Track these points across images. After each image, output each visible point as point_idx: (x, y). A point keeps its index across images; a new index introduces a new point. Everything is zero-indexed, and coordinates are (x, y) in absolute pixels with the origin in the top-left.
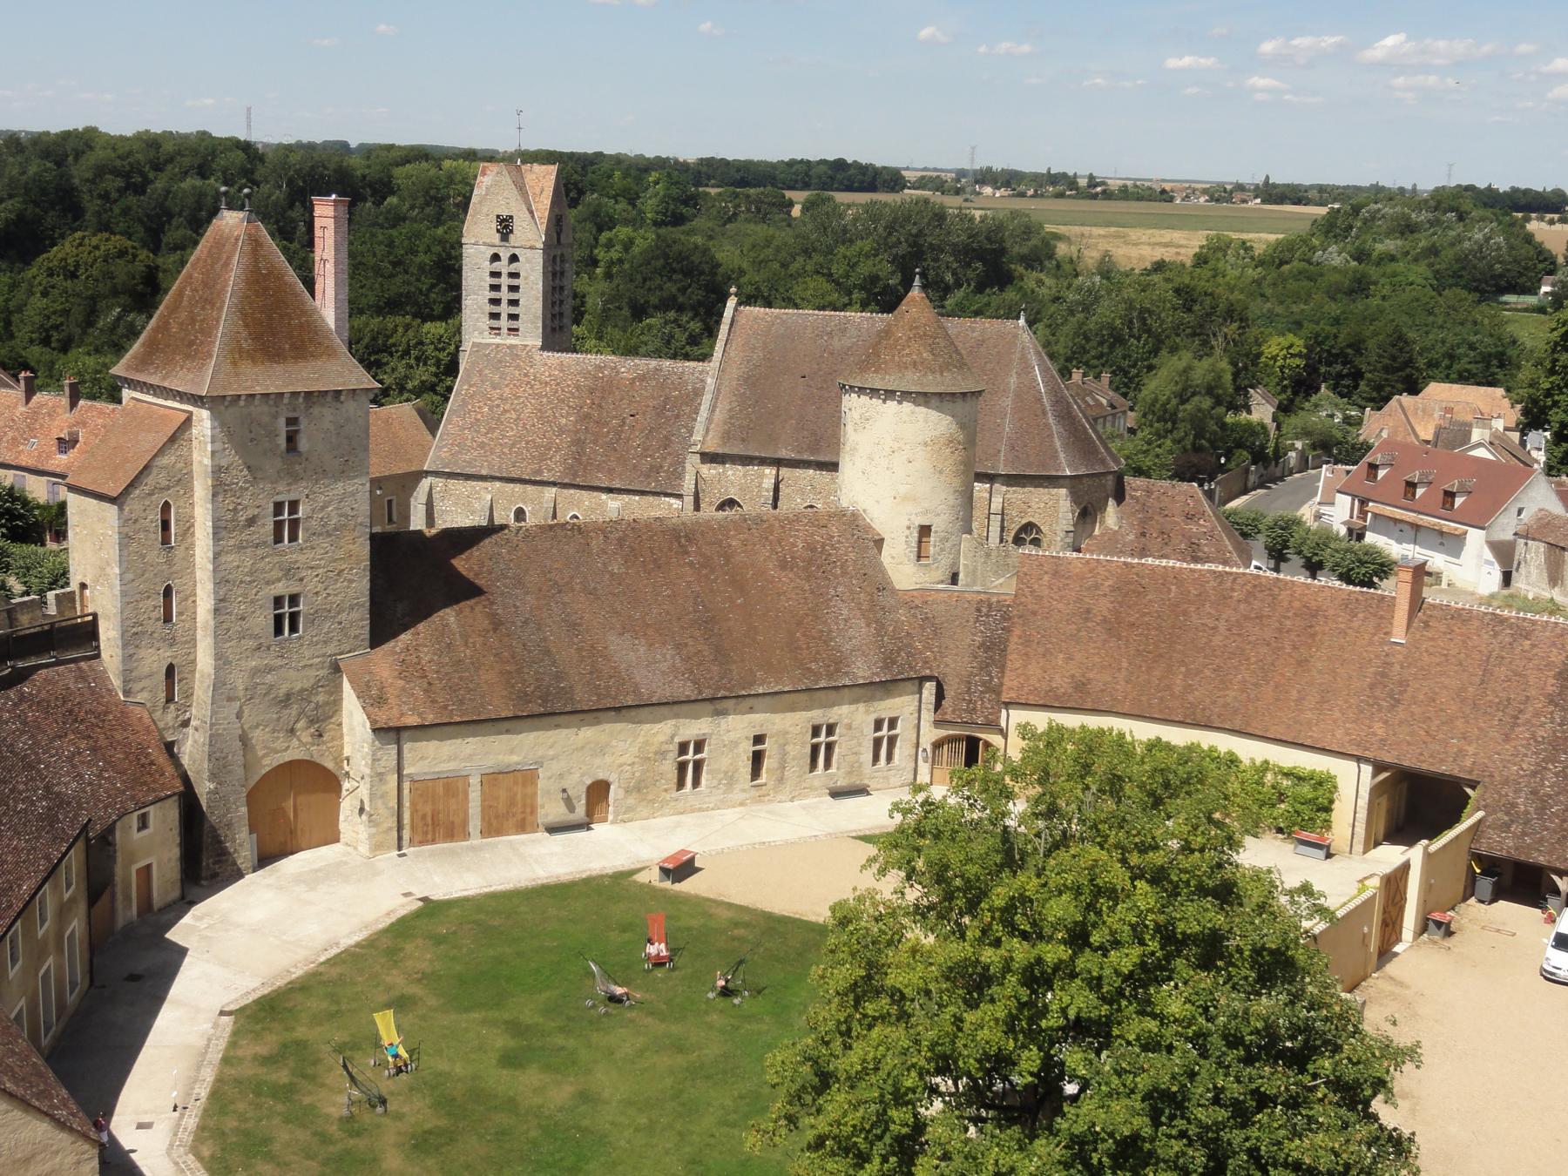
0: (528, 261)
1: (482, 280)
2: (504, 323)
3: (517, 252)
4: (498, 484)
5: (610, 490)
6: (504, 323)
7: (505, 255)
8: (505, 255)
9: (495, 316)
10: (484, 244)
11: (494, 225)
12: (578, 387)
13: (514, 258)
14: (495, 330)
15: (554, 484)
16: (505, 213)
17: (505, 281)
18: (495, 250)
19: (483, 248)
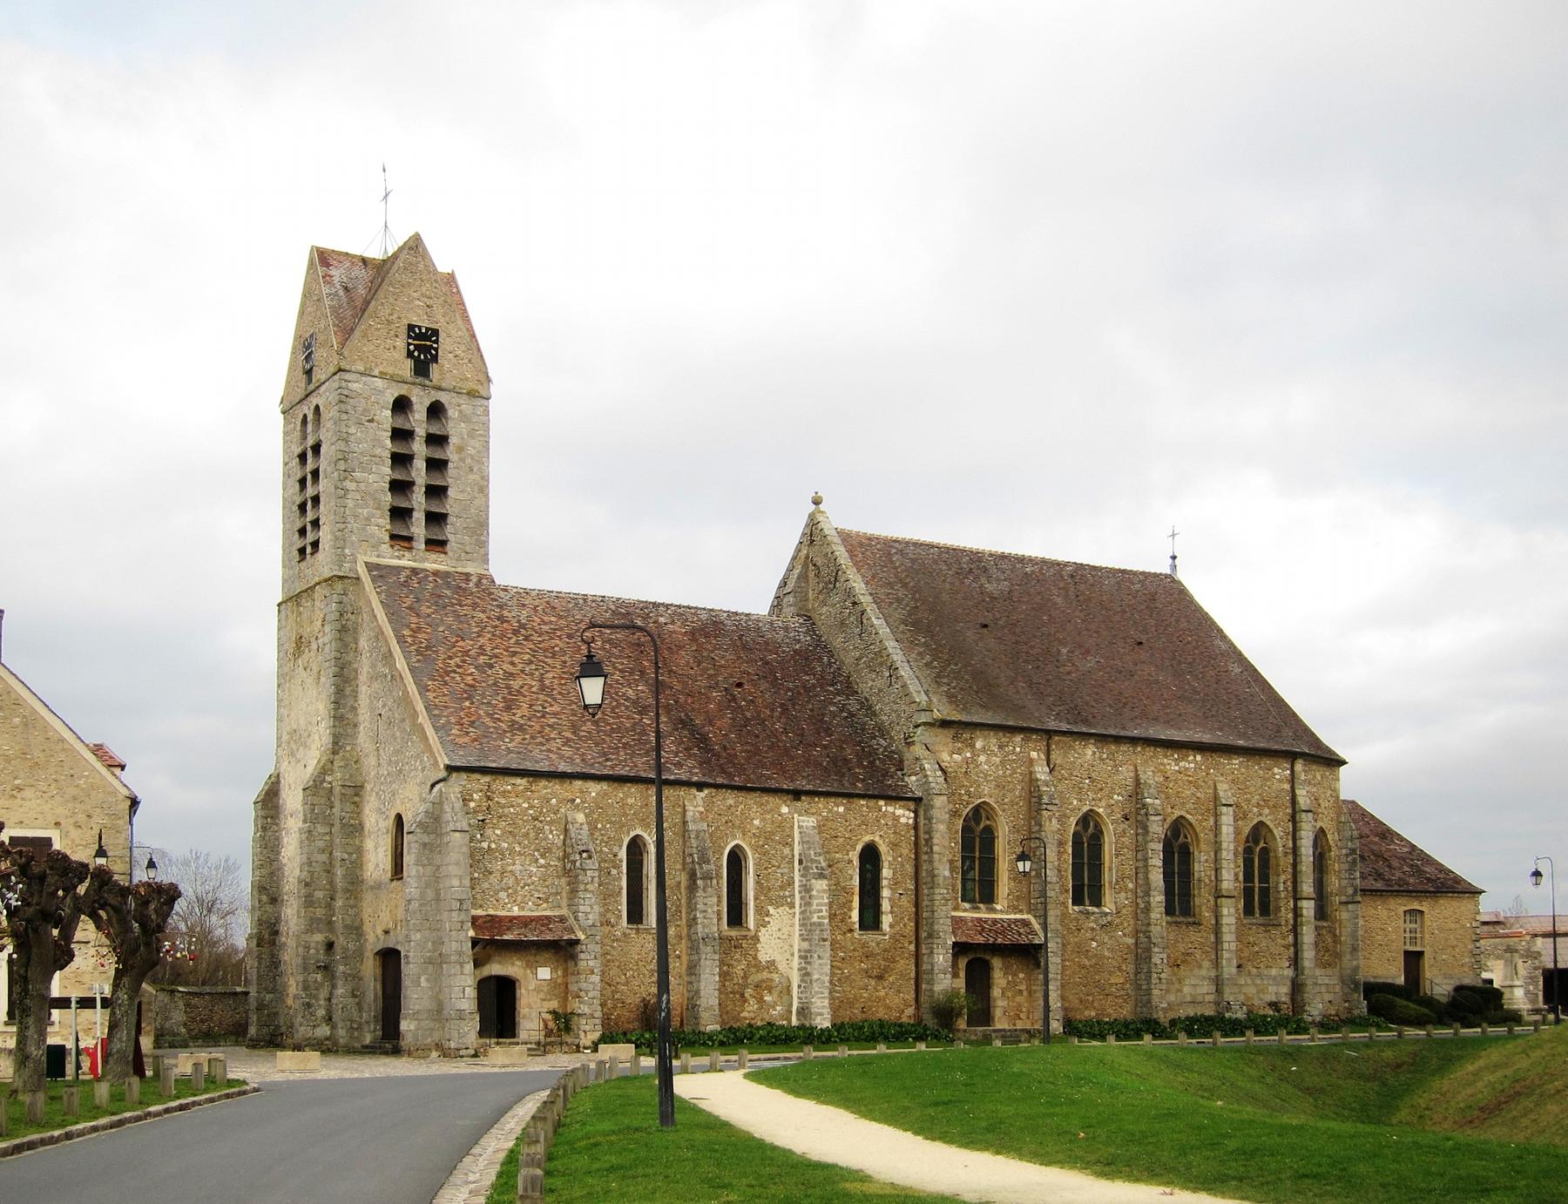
0: (464, 418)
1: (377, 442)
2: (418, 527)
3: (443, 398)
4: (594, 789)
5: (797, 795)
6: (418, 527)
7: (420, 403)
8: (420, 403)
9: (400, 514)
10: (382, 375)
11: (401, 343)
12: (609, 641)
13: (436, 411)
14: (401, 540)
15: (700, 786)
16: (424, 323)
17: (419, 448)
18: (402, 390)
19: (379, 383)
